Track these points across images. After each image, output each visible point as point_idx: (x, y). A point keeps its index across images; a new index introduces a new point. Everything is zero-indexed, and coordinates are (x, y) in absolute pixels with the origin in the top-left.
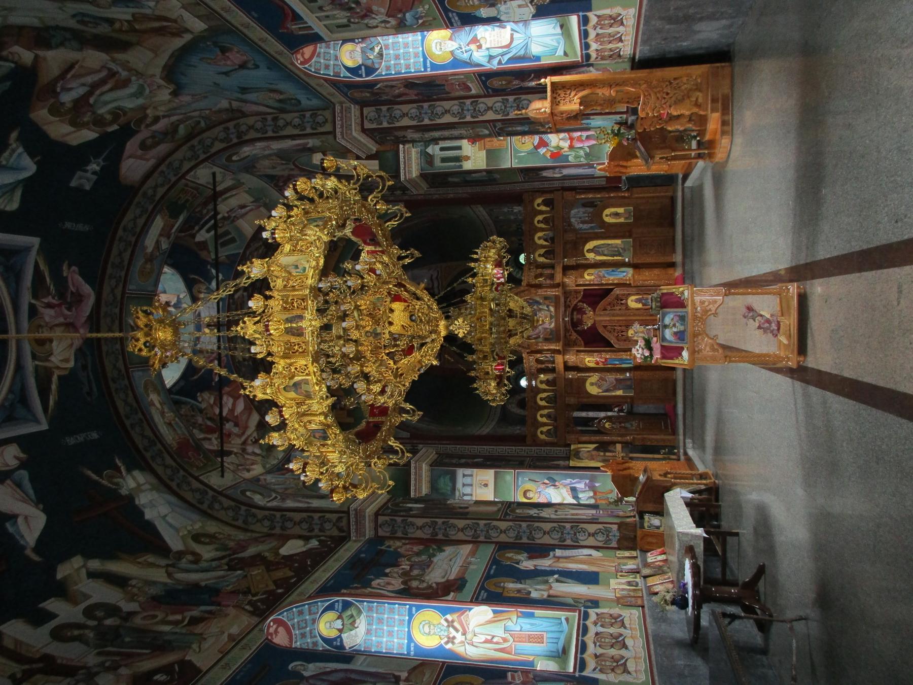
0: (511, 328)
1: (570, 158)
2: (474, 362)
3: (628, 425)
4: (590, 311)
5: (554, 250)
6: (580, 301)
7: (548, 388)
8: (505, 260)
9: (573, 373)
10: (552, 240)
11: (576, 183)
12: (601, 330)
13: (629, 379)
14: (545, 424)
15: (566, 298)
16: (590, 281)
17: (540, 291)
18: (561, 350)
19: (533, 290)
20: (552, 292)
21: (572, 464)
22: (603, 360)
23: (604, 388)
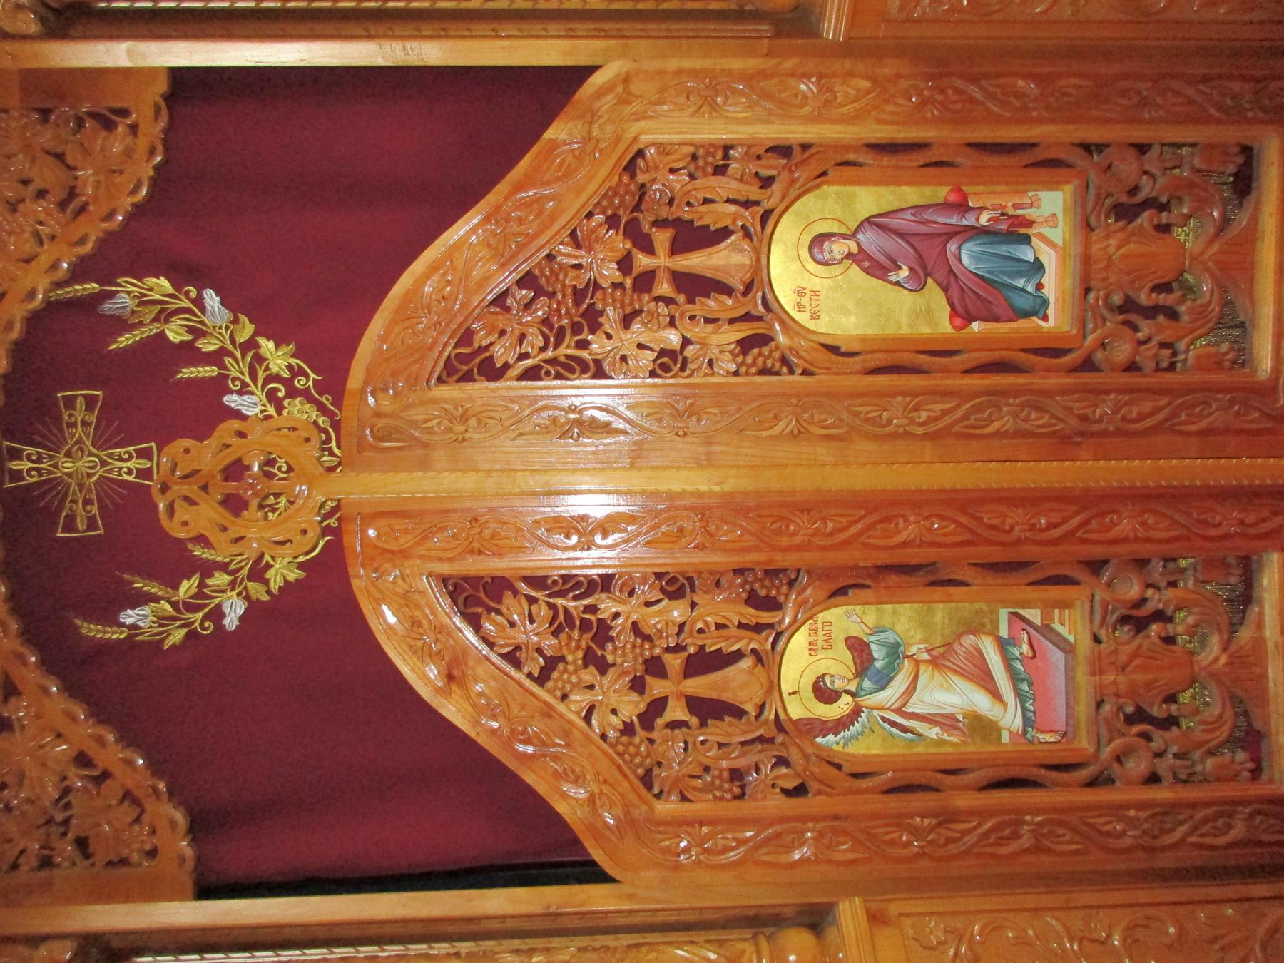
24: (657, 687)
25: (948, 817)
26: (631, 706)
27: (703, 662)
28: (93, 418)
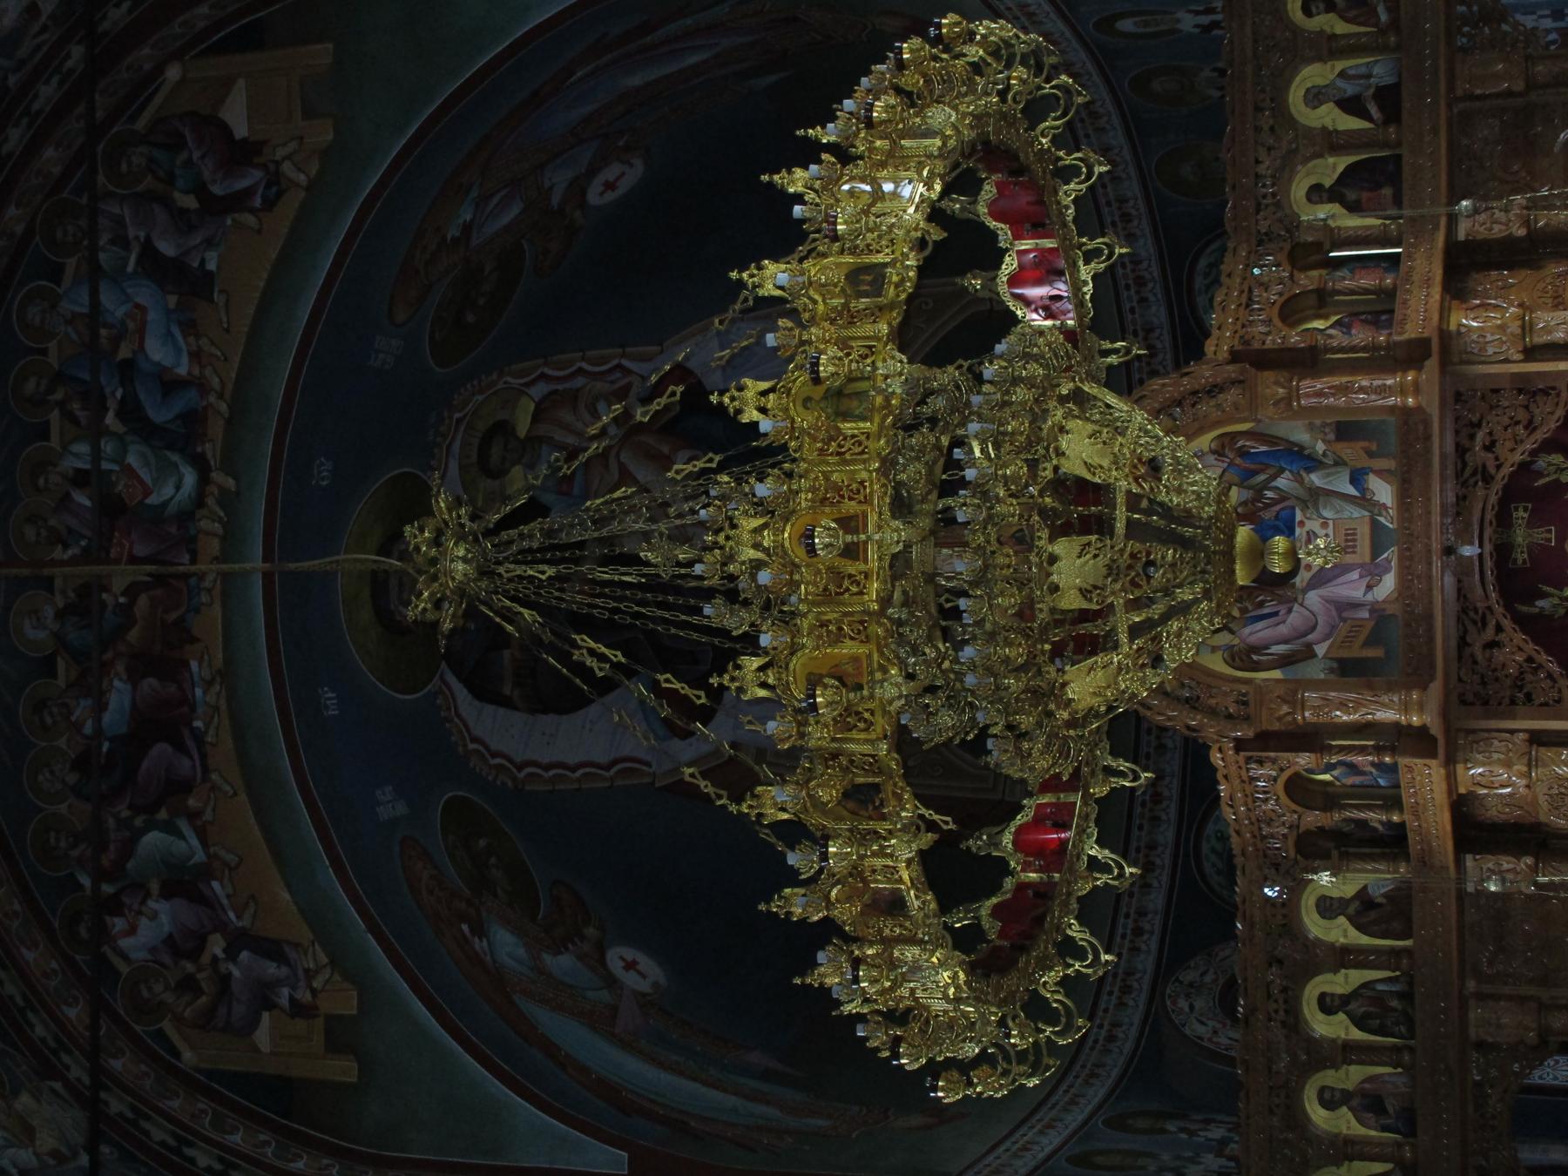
0: (1071, 601)
2: (794, 832)
5: (1398, 159)
6: (1548, 446)
7: (1365, 940)
8: (1070, 192)
9: (1507, 863)
10: (1389, 99)
15: (1466, 429)
17: (1308, 385)
18: (1436, 730)
19: (1271, 385)
20: (1383, 391)
28: (1526, 515)
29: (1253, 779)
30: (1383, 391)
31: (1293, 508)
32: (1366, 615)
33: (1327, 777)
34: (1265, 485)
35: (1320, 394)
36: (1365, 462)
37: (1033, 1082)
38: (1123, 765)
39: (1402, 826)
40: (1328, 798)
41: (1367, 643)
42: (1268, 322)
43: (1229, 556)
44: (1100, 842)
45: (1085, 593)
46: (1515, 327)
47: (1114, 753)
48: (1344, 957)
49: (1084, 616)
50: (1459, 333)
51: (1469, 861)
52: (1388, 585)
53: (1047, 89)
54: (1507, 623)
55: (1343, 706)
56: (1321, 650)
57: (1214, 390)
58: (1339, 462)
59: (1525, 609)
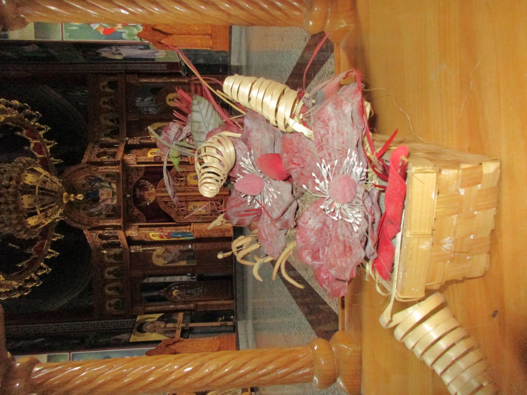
1: (124, 36)
3: (193, 291)
4: (152, 188)
6: (142, 178)
8: (41, 133)
11: (138, 67)
12: (162, 206)
13: (191, 250)
14: (111, 297)
16: (150, 159)
17: (100, 168)
18: (122, 226)
19: (93, 168)
20: (113, 169)
21: (134, 338)
22: (167, 234)
23: (170, 259)
24: (179, 209)
25: (199, 218)
26: (177, 210)
27: (182, 207)
29: (92, 236)
30: (113, 169)
31: (98, 189)
32: (111, 207)
33: (107, 234)
34: (94, 185)
35: (102, 169)
36: (111, 181)
37: (26, 294)
38: (58, 235)
39: (119, 242)
40: (107, 238)
41: (112, 211)
42: (94, 157)
43: (62, 197)
44: (51, 248)
45: (29, 205)
46: (134, 159)
47: (56, 233)
48: (112, 265)
49: (32, 209)
50: (125, 160)
51: (131, 247)
52: (115, 202)
53: (34, 114)
54: (135, 208)
55: (106, 222)
56: (104, 213)
57: (83, 168)
58: (107, 181)
59: (139, 205)
